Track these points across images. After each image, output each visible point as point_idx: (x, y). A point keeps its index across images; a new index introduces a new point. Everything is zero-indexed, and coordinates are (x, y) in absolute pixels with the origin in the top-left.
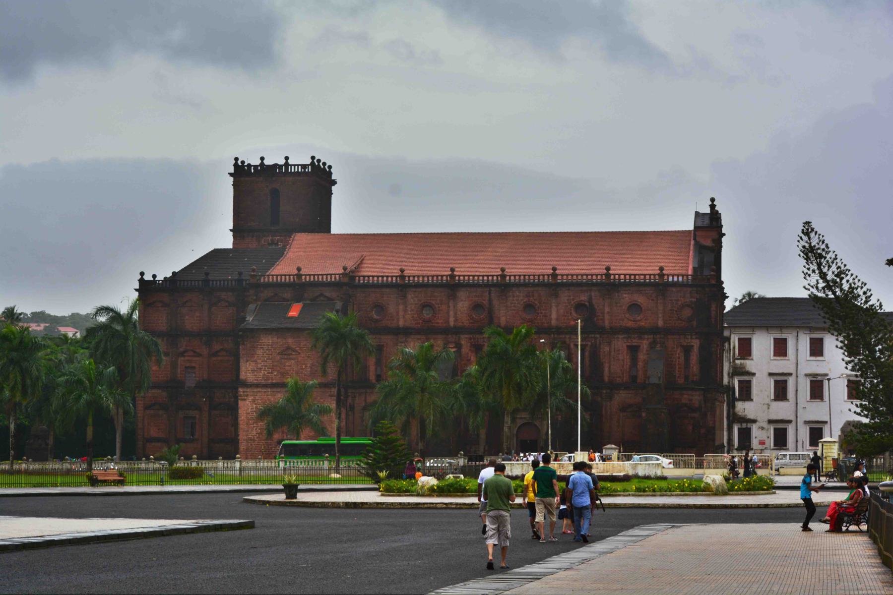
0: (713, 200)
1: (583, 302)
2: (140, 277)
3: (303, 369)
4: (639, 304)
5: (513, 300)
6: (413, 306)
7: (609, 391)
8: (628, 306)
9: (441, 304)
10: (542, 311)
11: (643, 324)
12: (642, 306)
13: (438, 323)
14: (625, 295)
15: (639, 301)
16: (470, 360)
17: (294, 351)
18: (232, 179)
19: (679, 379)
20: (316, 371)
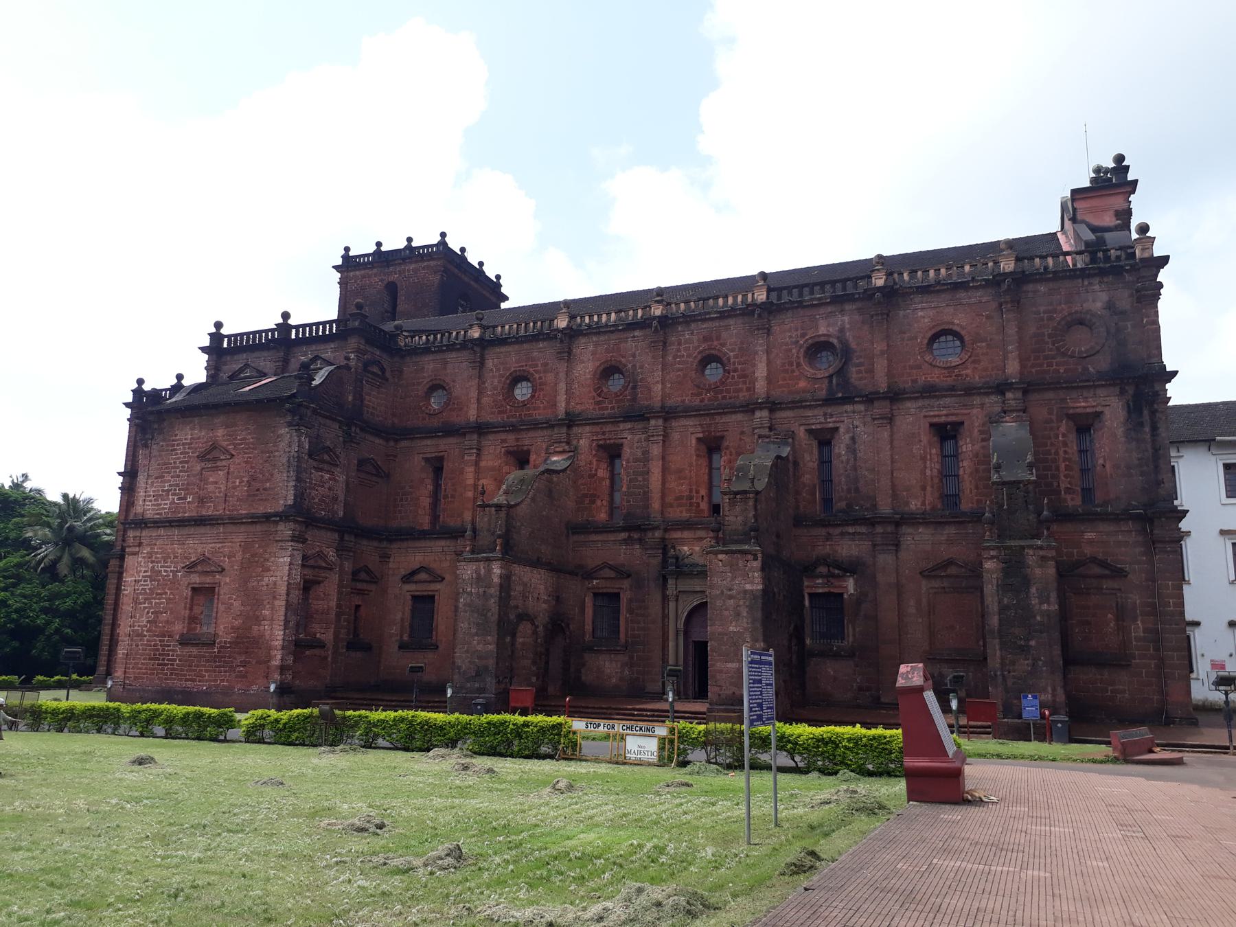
1: (822, 339)
2: (137, 386)
3: (235, 488)
4: (956, 328)
6: (496, 381)
7: (890, 529)
8: (929, 334)
9: (545, 372)
10: (736, 366)
11: (969, 371)
12: (963, 333)
13: (539, 408)
14: (920, 314)
15: (956, 321)
16: (596, 475)
17: (224, 453)
18: (339, 275)
19: (1069, 497)
20: (258, 490)
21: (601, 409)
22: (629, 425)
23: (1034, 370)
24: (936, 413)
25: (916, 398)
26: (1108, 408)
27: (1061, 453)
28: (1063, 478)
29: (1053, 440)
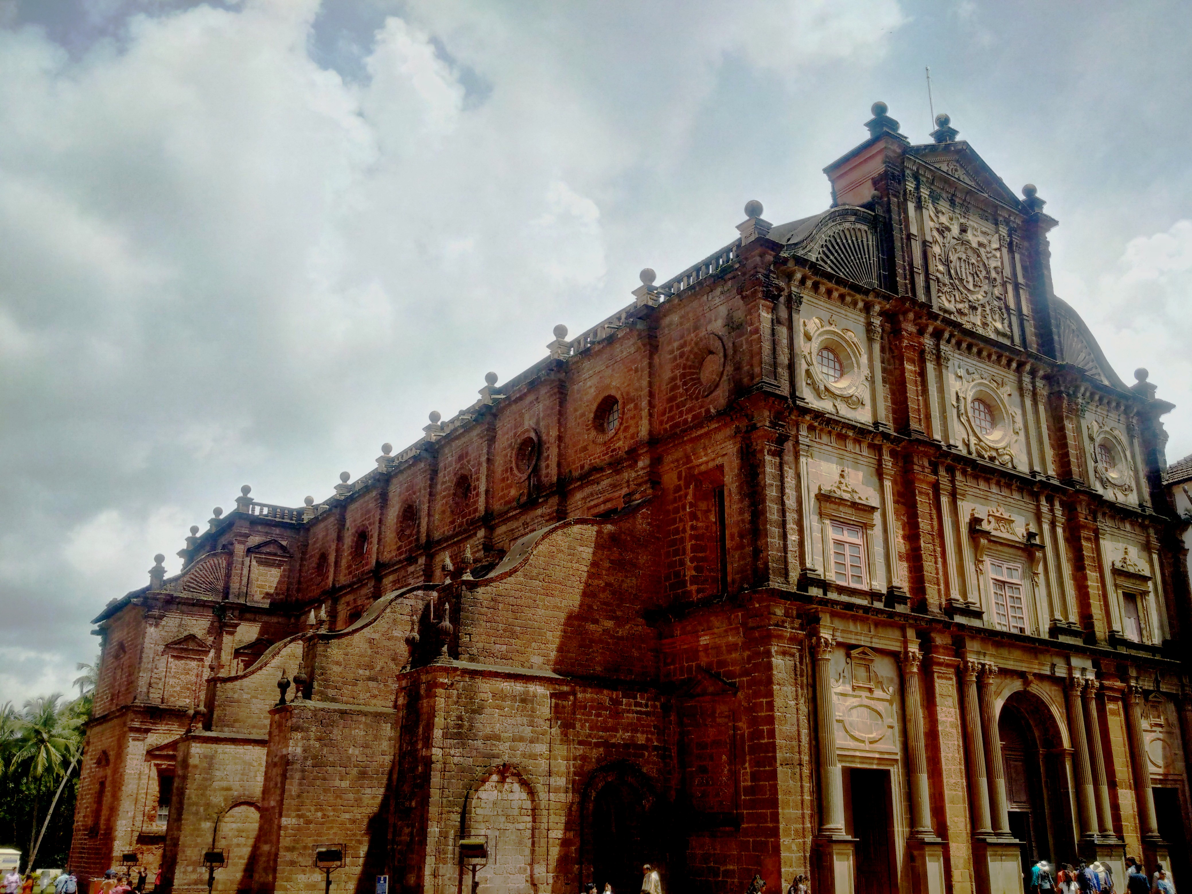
1: (526, 436)
4: (613, 393)
5: (445, 477)
8: (594, 407)
11: (620, 444)
12: (618, 396)
14: (589, 384)
19: (694, 588)
21: (401, 554)
22: (411, 569)
23: (668, 426)
24: (595, 502)
25: (581, 488)
26: (726, 458)
27: (688, 528)
28: (689, 563)
29: (681, 513)
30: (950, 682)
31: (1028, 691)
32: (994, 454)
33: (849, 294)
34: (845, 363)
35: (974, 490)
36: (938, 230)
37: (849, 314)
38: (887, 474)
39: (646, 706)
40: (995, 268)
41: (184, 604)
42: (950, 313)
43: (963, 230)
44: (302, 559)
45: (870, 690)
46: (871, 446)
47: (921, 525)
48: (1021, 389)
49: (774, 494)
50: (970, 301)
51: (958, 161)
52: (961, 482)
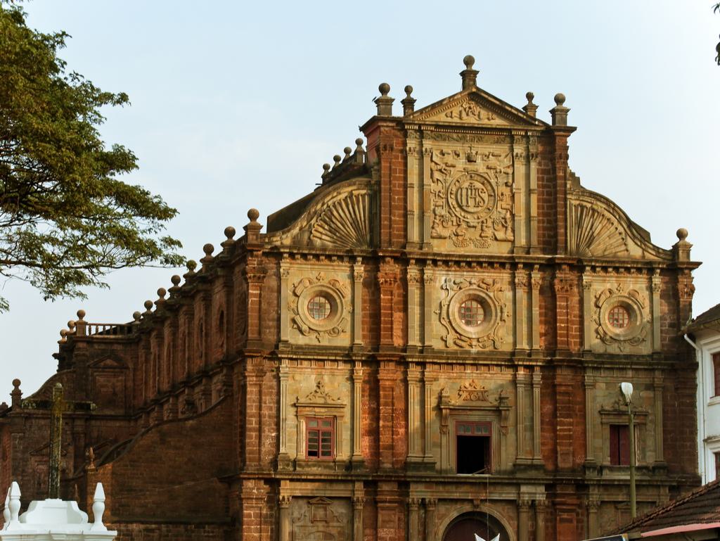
0: (469, 61)
30: (394, 512)
31: (476, 512)
32: (474, 343)
33: (334, 256)
34: (333, 303)
35: (448, 374)
36: (440, 171)
37: (336, 268)
38: (357, 379)
39: (213, 532)
40: (506, 183)
41: (39, 418)
42: (445, 238)
43: (470, 160)
44: (135, 370)
45: (326, 521)
46: (345, 362)
47: (382, 411)
48: (513, 285)
49: (254, 411)
50: (467, 222)
51: (472, 100)
52: (430, 372)
